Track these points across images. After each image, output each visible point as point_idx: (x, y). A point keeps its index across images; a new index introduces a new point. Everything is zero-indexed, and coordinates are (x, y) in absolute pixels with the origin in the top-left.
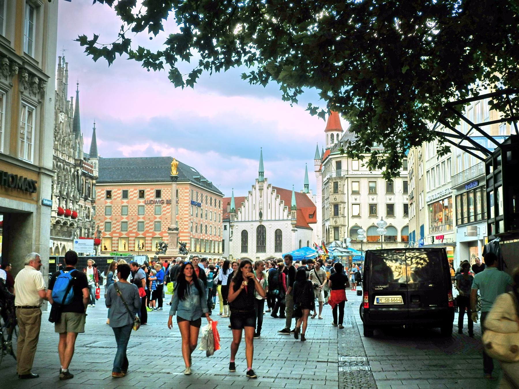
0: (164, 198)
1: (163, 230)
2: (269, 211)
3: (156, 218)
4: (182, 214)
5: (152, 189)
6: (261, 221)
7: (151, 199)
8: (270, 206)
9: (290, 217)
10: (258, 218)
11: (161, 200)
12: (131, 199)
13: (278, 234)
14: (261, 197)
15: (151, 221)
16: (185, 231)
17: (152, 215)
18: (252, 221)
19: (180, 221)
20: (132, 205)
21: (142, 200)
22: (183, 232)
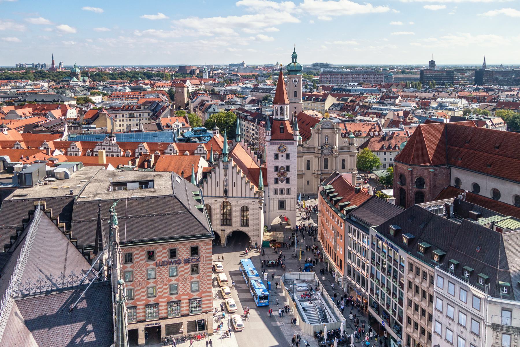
0: (180, 258)
1: (181, 293)
2: (235, 189)
3: (171, 281)
4: (204, 273)
5: (164, 249)
6: (226, 197)
7: (164, 260)
8: (234, 185)
9: (257, 196)
10: (222, 194)
11: (176, 259)
12: (138, 262)
13: (244, 209)
14: (226, 175)
15: (166, 285)
16: (208, 290)
17: (166, 277)
18: (216, 197)
19: (202, 280)
20: (139, 270)
21: (152, 263)
22: (206, 292)
